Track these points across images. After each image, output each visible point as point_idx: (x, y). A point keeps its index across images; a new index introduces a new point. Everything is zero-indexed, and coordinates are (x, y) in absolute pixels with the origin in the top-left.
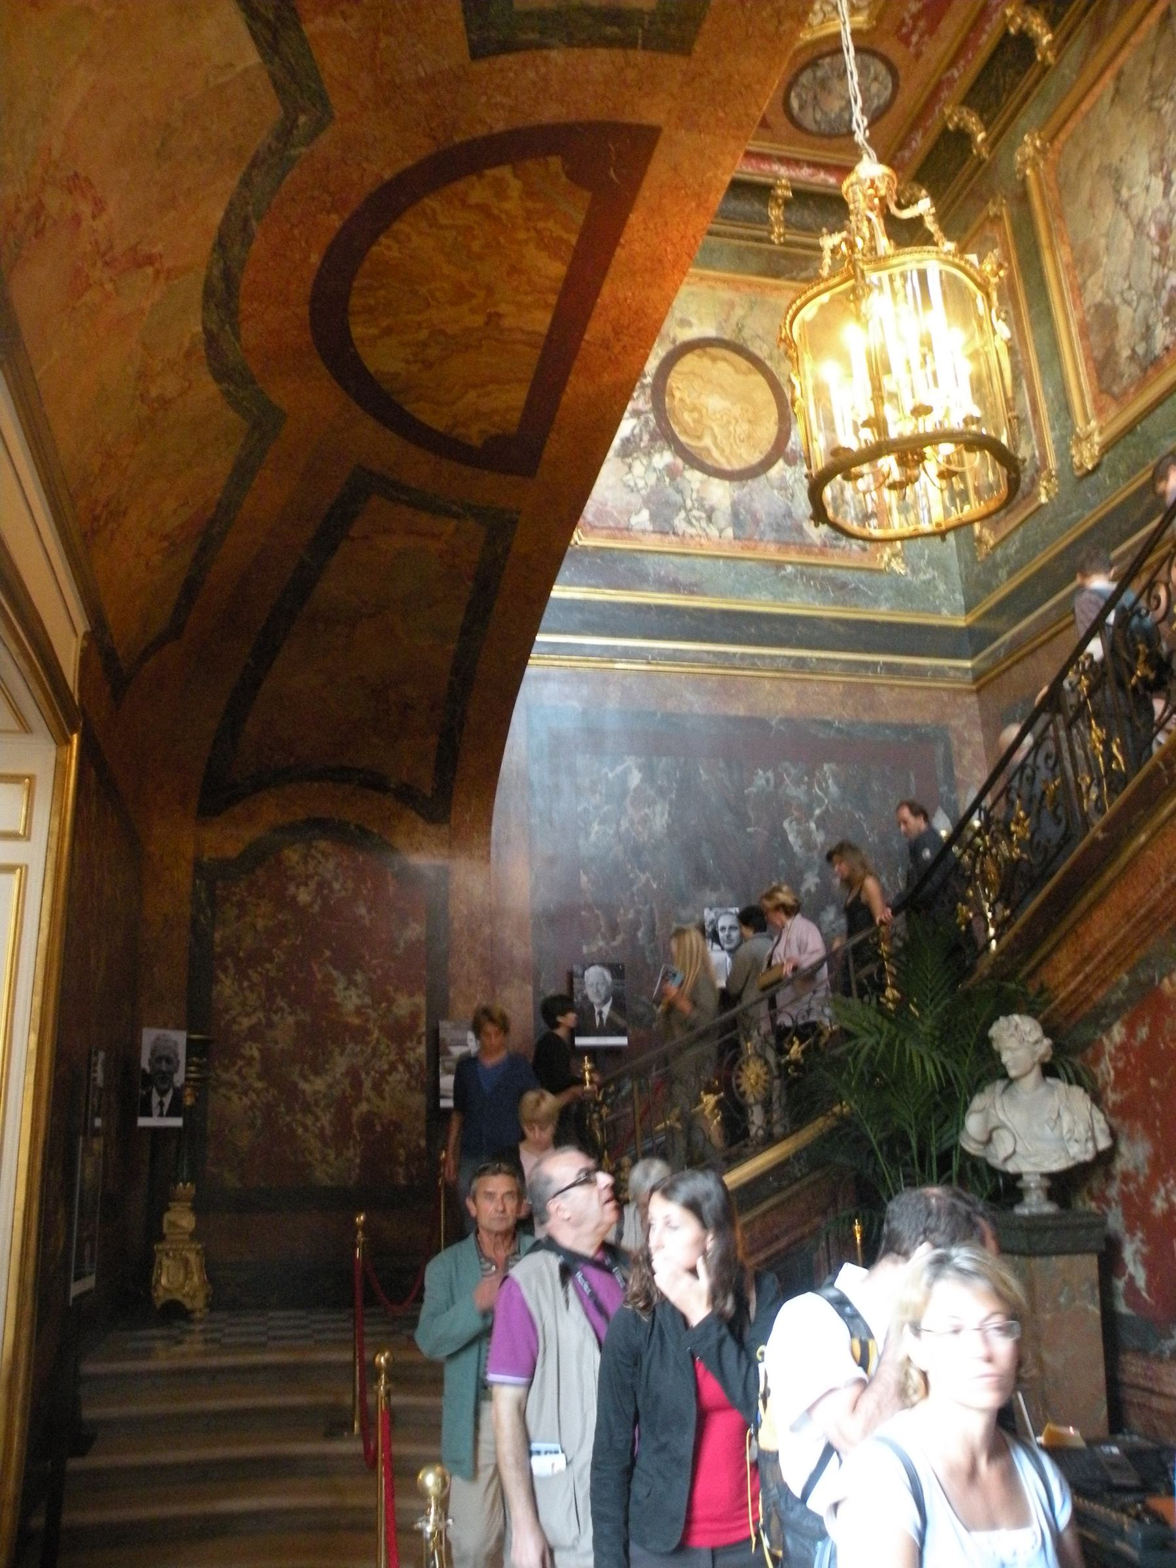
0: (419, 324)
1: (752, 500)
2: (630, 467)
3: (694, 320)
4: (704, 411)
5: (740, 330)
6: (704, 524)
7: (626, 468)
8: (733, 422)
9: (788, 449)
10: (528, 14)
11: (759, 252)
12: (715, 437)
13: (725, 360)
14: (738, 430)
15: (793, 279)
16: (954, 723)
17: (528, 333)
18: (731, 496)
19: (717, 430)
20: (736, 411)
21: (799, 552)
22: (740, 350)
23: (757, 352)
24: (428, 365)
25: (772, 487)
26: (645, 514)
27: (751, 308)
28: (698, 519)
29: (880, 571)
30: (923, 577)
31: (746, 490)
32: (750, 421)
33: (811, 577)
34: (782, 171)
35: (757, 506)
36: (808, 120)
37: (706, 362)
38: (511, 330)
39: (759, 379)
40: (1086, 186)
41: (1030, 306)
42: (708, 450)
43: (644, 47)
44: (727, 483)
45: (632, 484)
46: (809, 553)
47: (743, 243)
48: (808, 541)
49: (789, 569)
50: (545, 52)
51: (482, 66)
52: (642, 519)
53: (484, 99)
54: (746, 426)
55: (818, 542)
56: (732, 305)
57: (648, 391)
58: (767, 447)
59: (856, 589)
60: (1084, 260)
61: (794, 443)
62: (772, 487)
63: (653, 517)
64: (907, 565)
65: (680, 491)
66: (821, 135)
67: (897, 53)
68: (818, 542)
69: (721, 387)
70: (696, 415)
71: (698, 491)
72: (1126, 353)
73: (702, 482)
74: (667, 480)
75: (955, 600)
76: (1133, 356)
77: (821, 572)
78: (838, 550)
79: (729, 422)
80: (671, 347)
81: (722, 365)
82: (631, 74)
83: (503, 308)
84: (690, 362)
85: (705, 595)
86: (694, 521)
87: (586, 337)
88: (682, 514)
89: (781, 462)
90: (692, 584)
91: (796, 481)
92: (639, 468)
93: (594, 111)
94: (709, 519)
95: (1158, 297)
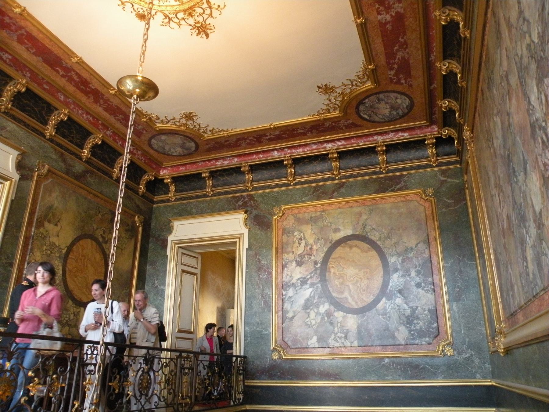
1: (368, 323)
2: (309, 313)
3: (341, 228)
4: (345, 278)
5: (364, 227)
6: (343, 340)
7: (307, 315)
8: (360, 280)
9: (388, 291)
11: (375, 179)
12: (350, 291)
13: (356, 246)
14: (363, 284)
15: (393, 191)
18: (357, 323)
19: (351, 286)
20: (361, 274)
22: (363, 238)
23: (373, 238)
25: (379, 315)
26: (315, 339)
27: (370, 214)
28: (340, 338)
30: (465, 356)
31: (365, 318)
32: (368, 279)
33: (399, 364)
34: (379, 138)
35: (370, 326)
36: (377, 119)
37: (347, 249)
39: (374, 253)
42: (346, 298)
44: (355, 316)
45: (309, 323)
47: (367, 178)
49: (387, 360)
52: (313, 342)
54: (366, 282)
56: (360, 214)
57: (318, 271)
58: (376, 291)
59: (424, 368)
61: (391, 287)
62: (379, 315)
63: (319, 340)
64: (454, 350)
65: (332, 324)
66: (389, 121)
67: (399, 88)
69: (353, 261)
70: (341, 280)
71: (341, 323)
73: (343, 317)
74: (326, 318)
75: (485, 368)
77: (404, 360)
79: (357, 281)
80: (330, 245)
81: (354, 249)
84: (339, 251)
85: (342, 380)
86: (338, 339)
88: (333, 336)
89: (384, 299)
90: (336, 374)
91: (391, 309)
92: (313, 315)
94: (346, 337)
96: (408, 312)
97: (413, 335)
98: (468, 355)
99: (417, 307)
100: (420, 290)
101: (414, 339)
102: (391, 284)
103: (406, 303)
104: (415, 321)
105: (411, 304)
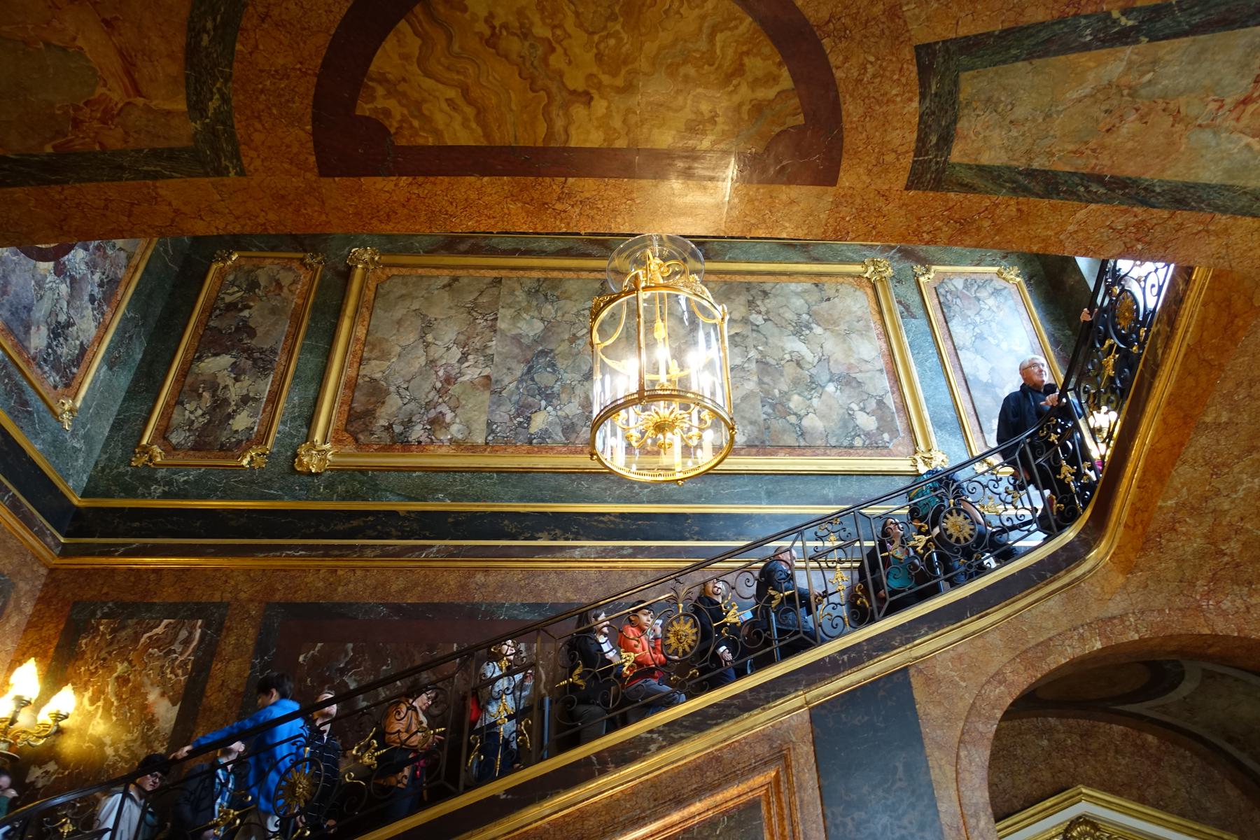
0: (560, 26)
1: (14, 271)
10: (956, 83)
16: (21, 584)
17: (566, 131)
21: (14, 346)
24: (492, 41)
29: (54, 413)
35: (13, 279)
38: (567, 115)
40: (399, 312)
41: (307, 336)
43: (915, 162)
46: (20, 354)
48: (26, 344)
50: (917, 99)
51: (908, 53)
53: (872, 59)
55: (32, 351)
59: (30, 413)
60: (371, 346)
68: (32, 351)
72: (383, 422)
76: (389, 428)
78: (39, 371)
82: (890, 158)
83: (600, 106)
87: (571, 180)
89: (51, 264)
91: (51, 289)
93: (853, 140)
95: (428, 411)
96: (62, 318)
97: (49, 354)
98: (77, 446)
99: (74, 324)
100: (90, 306)
101: (45, 361)
102: (70, 256)
103: (68, 303)
104: (61, 339)
105: (72, 312)
